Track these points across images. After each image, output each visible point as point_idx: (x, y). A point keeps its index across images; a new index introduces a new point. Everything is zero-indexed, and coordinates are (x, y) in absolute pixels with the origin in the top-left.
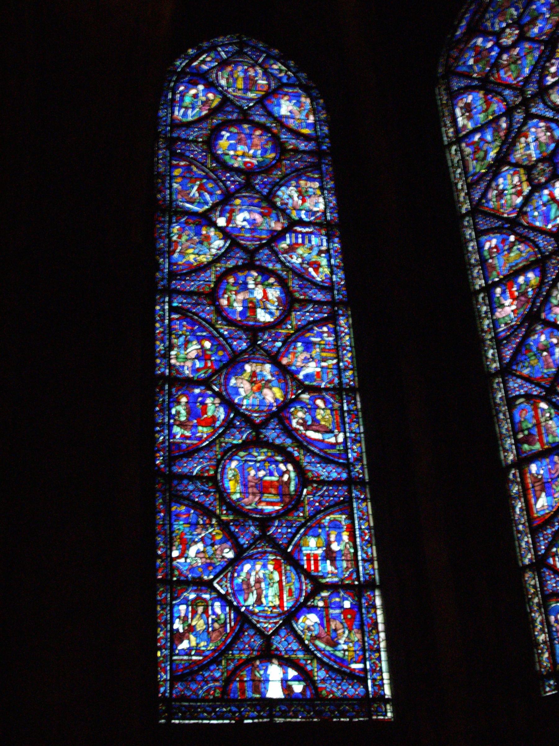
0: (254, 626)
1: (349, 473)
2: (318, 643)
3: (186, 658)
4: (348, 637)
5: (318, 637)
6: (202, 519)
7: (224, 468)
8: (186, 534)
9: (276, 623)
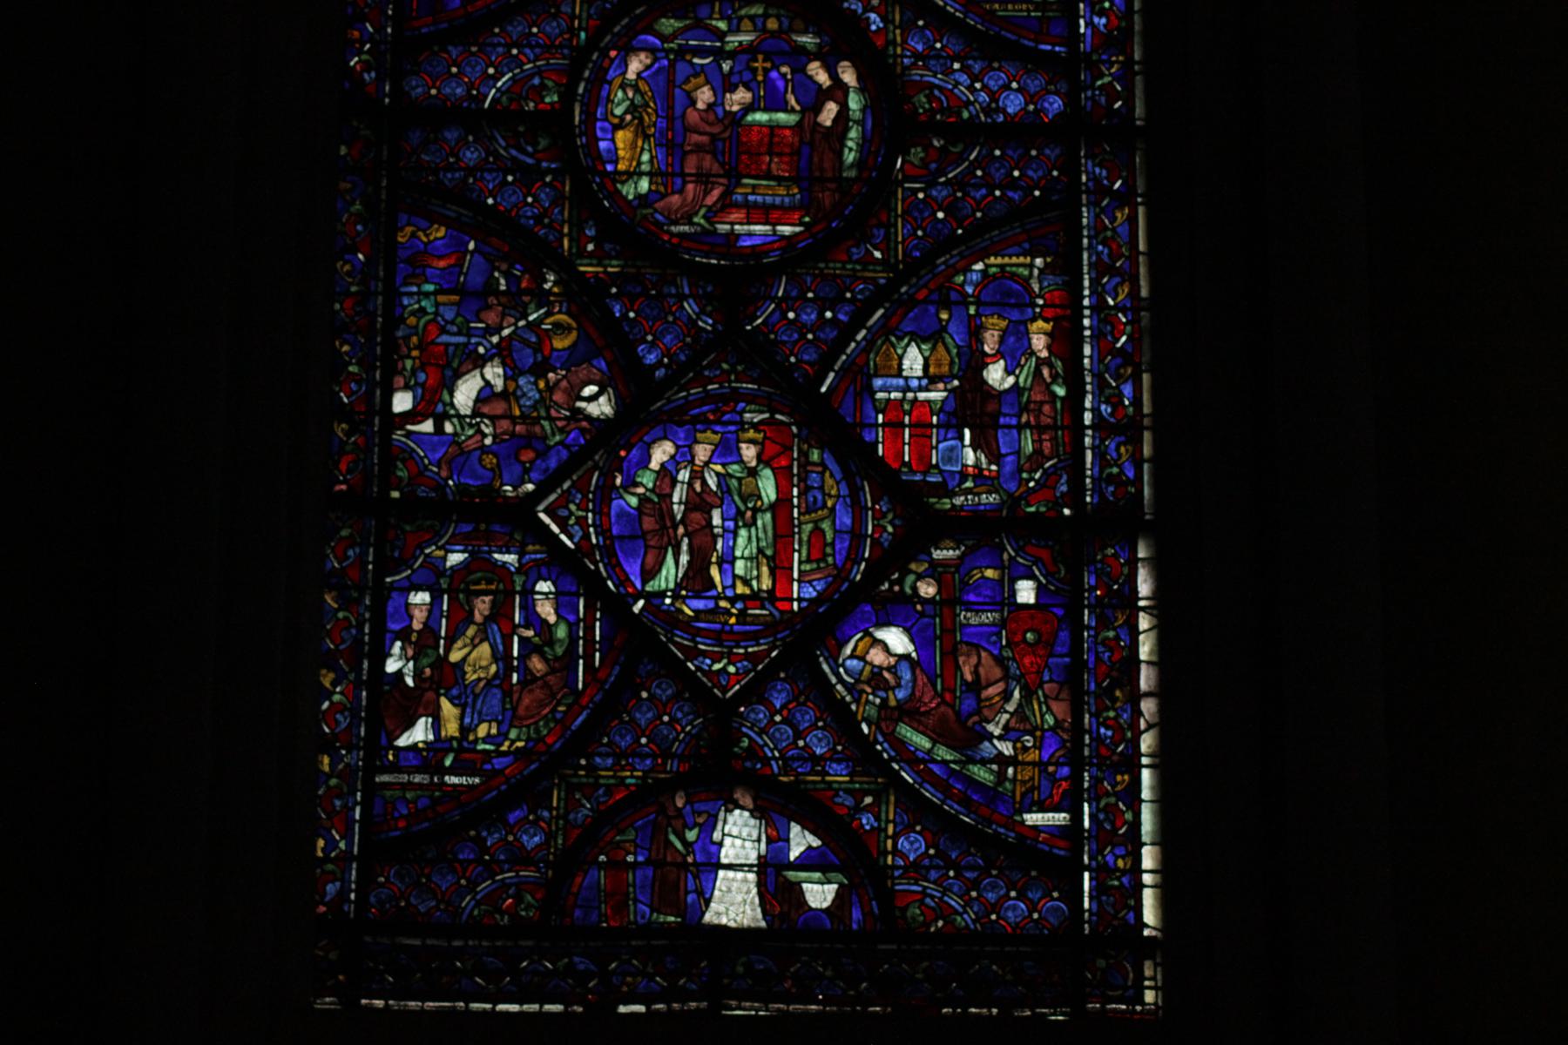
0: (675, 670)
1: (1071, 99)
2: (906, 732)
3: (417, 779)
4: (1019, 713)
5: (909, 712)
6: (508, 275)
7: (600, 80)
8: (443, 331)
9: (754, 658)
